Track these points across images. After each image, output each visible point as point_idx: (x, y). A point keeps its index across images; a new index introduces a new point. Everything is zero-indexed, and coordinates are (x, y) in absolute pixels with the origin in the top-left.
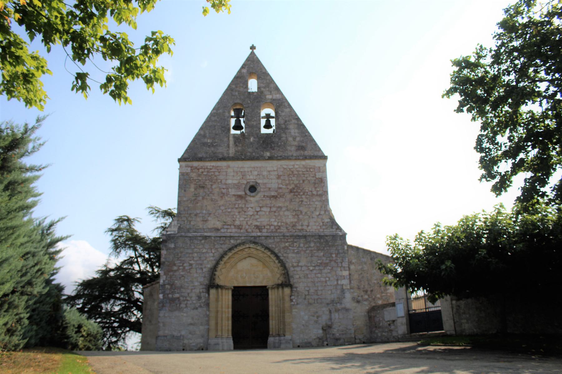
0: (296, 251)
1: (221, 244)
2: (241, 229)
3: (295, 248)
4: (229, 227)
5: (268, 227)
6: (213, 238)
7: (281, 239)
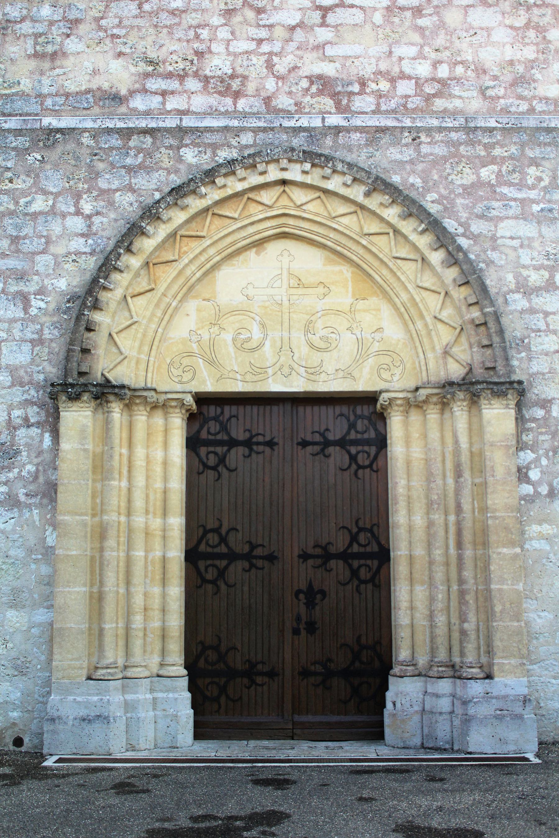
0: (536, 208)
1: (130, 170)
2: (237, 95)
3: (533, 194)
4: (174, 85)
5: (384, 86)
6: (86, 140)
7: (457, 144)
